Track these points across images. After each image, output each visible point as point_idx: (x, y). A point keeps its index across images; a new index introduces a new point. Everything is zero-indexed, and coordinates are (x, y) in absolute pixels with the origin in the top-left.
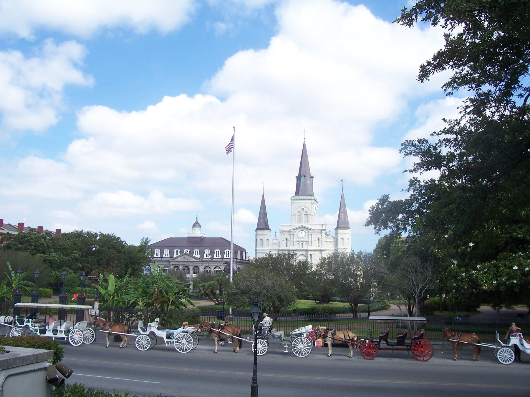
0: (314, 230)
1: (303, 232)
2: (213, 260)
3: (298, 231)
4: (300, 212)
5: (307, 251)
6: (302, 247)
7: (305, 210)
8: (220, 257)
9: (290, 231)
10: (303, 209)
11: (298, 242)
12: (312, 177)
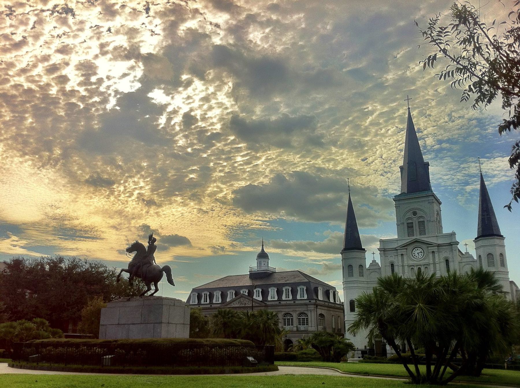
0: (439, 246)
1: (420, 250)
2: (282, 303)
3: (410, 248)
8: (291, 297)
9: (396, 249)
10: (415, 214)
12: (427, 165)
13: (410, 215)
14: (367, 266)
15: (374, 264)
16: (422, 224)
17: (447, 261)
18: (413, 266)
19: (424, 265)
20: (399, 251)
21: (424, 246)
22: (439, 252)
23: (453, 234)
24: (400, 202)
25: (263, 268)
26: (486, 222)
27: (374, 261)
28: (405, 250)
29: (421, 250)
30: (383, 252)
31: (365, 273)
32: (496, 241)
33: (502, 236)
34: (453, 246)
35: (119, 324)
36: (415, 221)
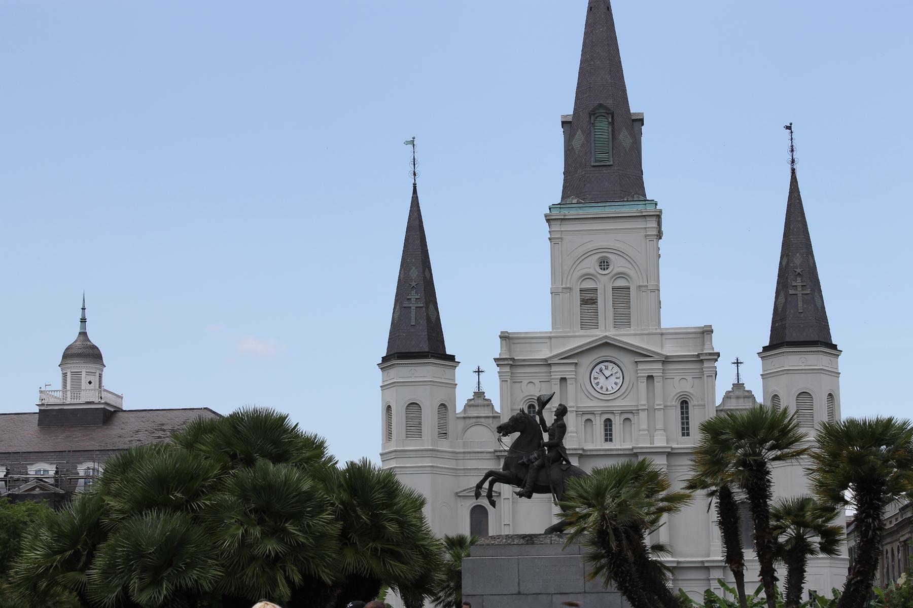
0: (666, 361)
1: (611, 369)
3: (586, 362)
4: (588, 277)
6: (608, 437)
7: (618, 264)
9: (547, 363)
10: (604, 264)
13: (591, 265)
14: (460, 408)
15: (480, 402)
16: (622, 294)
17: (684, 404)
18: (593, 413)
19: (623, 412)
20: (554, 369)
21: (626, 361)
22: (665, 378)
23: (706, 332)
24: (567, 227)
25: (87, 396)
26: (800, 304)
27: (479, 394)
28: (572, 368)
29: (616, 369)
30: (507, 369)
31: (453, 427)
32: (814, 359)
33: (834, 347)
34: (706, 364)
35: (519, 593)
36: (604, 287)
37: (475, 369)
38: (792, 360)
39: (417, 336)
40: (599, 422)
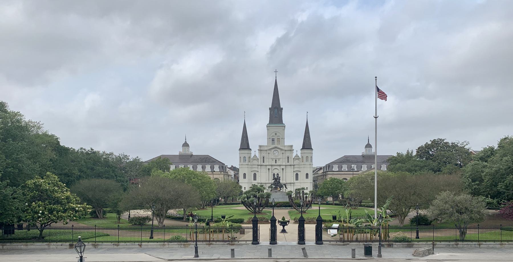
0: (285, 151)
3: (273, 150)
4: (273, 136)
5: (280, 166)
9: (266, 150)
10: (276, 134)
11: (272, 159)
12: (282, 109)
13: (274, 134)
21: (279, 150)
23: (292, 146)
36: (276, 138)
37: (255, 151)
38: (306, 151)
39: (245, 145)
40: (274, 160)
